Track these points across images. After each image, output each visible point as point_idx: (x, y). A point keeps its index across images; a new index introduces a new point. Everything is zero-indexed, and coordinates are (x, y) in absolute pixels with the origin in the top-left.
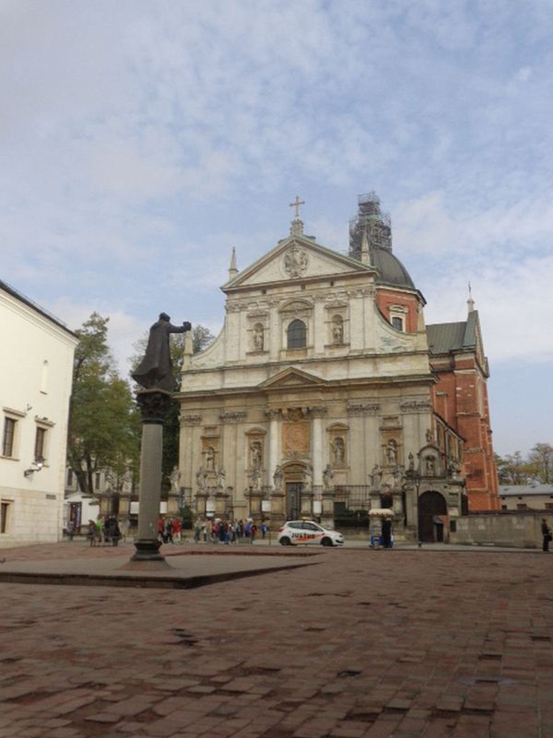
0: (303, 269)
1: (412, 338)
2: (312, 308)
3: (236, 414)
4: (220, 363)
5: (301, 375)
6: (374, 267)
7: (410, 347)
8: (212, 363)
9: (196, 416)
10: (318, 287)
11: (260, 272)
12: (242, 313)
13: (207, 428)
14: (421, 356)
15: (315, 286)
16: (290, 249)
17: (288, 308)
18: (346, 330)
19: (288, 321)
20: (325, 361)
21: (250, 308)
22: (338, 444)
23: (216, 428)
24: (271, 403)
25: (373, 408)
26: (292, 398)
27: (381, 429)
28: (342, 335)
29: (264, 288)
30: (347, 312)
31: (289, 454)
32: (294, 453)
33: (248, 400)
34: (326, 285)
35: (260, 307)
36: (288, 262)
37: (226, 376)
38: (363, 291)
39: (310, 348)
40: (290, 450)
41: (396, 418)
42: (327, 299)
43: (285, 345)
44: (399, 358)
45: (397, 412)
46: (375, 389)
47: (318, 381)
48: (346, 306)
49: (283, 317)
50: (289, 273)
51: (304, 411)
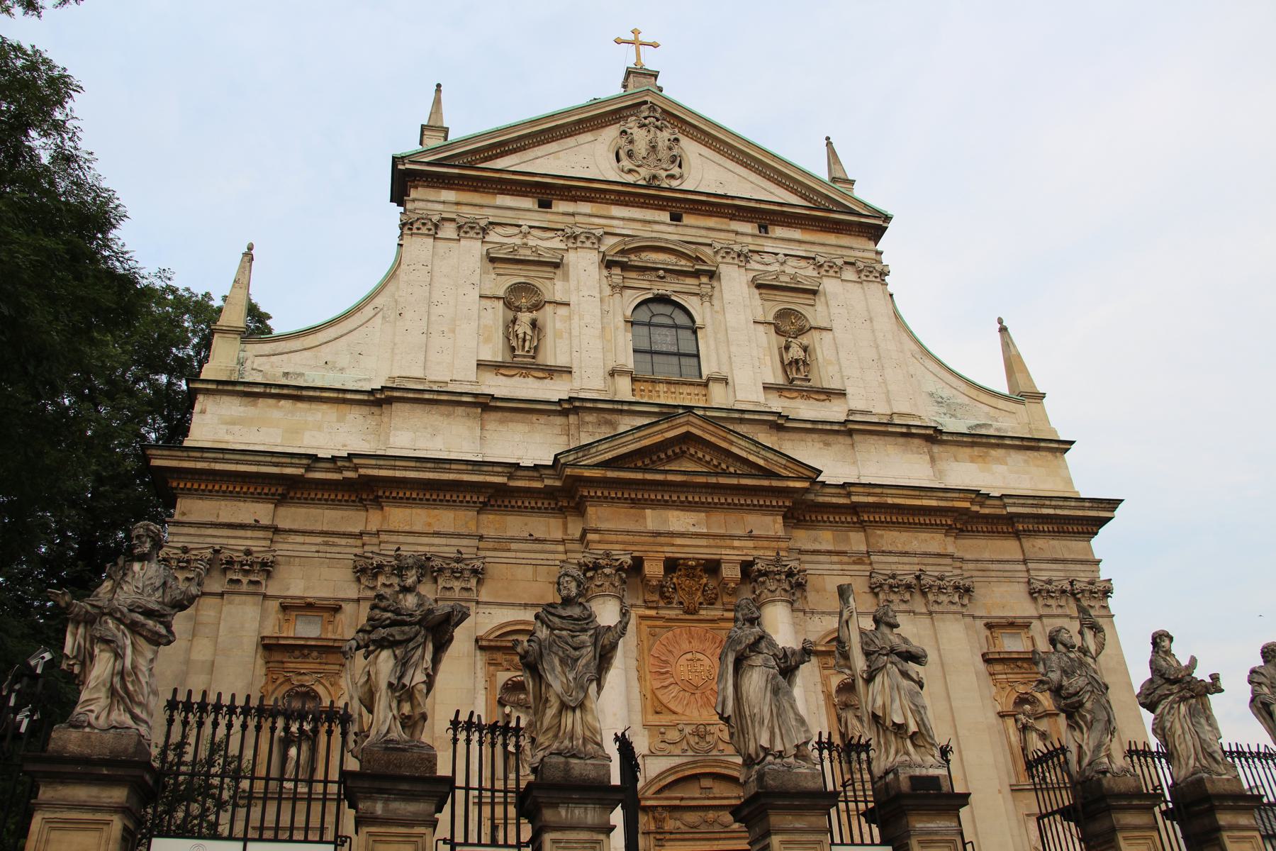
0: (672, 177)
1: (1011, 406)
2: (712, 275)
3: (437, 563)
4: (369, 380)
5: (724, 445)
7: (1013, 428)
8: (331, 374)
9: (248, 552)
10: (724, 227)
11: (531, 153)
12: (463, 242)
13: (292, 608)
14: (1049, 455)
15: (712, 222)
16: (634, 118)
17: (634, 259)
19: (629, 292)
20: (779, 424)
21: (493, 237)
22: (846, 706)
23: (336, 609)
24: (596, 531)
25: (957, 588)
26: (679, 521)
27: (987, 660)
30: (820, 307)
31: (673, 735)
32: (695, 733)
33: (488, 518)
35: (531, 243)
36: (630, 147)
37: (396, 421)
38: (860, 265)
39: (717, 380)
40: (674, 717)
41: (1027, 626)
43: (628, 361)
44: (995, 453)
45: (1022, 607)
46: (948, 530)
47: (784, 473)
48: (814, 292)
49: (617, 280)
51: (731, 572)
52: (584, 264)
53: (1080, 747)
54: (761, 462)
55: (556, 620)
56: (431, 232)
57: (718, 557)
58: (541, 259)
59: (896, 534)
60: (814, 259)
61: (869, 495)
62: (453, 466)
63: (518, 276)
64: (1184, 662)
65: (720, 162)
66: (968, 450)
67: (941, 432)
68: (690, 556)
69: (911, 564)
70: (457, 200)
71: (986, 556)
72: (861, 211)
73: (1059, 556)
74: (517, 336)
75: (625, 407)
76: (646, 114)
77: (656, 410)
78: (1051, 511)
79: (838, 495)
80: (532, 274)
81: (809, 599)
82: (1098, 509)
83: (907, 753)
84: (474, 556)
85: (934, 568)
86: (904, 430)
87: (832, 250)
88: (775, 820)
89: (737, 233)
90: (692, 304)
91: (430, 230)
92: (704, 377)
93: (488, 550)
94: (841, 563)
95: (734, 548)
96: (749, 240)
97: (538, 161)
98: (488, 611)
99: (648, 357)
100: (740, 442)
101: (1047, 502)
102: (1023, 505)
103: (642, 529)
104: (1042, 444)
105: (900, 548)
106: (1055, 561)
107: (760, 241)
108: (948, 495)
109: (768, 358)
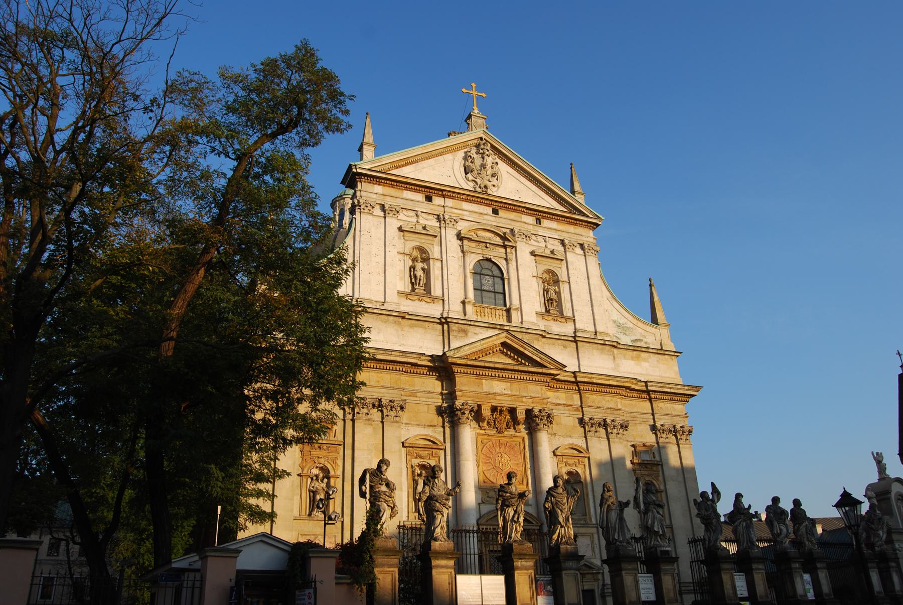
5: (522, 349)
6: (601, 217)
15: (513, 215)
18: (565, 296)
19: (473, 255)
21: (402, 216)
24: (461, 391)
28: (559, 303)
29: (430, 192)
34: (531, 220)
35: (422, 222)
38: (586, 246)
42: (536, 244)
43: (471, 294)
44: (644, 355)
50: (472, 184)
51: (521, 415)
52: (450, 235)
53: (709, 539)
54: (538, 360)
55: (556, 494)
56: (371, 212)
57: (515, 406)
58: (428, 233)
59: (594, 397)
60: (563, 241)
61: (586, 377)
62: (393, 353)
63: (415, 241)
64: (746, 506)
65: (518, 178)
66: (630, 353)
67: (619, 344)
68: (503, 405)
69: (601, 413)
70: (384, 193)
71: (635, 410)
72: (588, 214)
73: (670, 413)
74: (415, 277)
75: (472, 323)
76: (482, 147)
77: (487, 325)
78: (668, 390)
79: (571, 376)
80: (423, 241)
81: (554, 428)
82: (691, 390)
83: (658, 541)
84: (400, 399)
85: (611, 415)
86: (602, 342)
87: (571, 236)
88: (624, 565)
89: (525, 223)
90: (502, 264)
91: (370, 210)
92: (508, 306)
93: (407, 396)
94: (568, 410)
95: (523, 402)
96: (531, 227)
97: (424, 170)
98: (407, 428)
99: (479, 292)
100: (531, 349)
101: (668, 386)
102: (656, 386)
103: (481, 390)
104: (667, 353)
105: (597, 405)
106: (668, 415)
107: (537, 228)
108: (622, 380)
109: (538, 297)
